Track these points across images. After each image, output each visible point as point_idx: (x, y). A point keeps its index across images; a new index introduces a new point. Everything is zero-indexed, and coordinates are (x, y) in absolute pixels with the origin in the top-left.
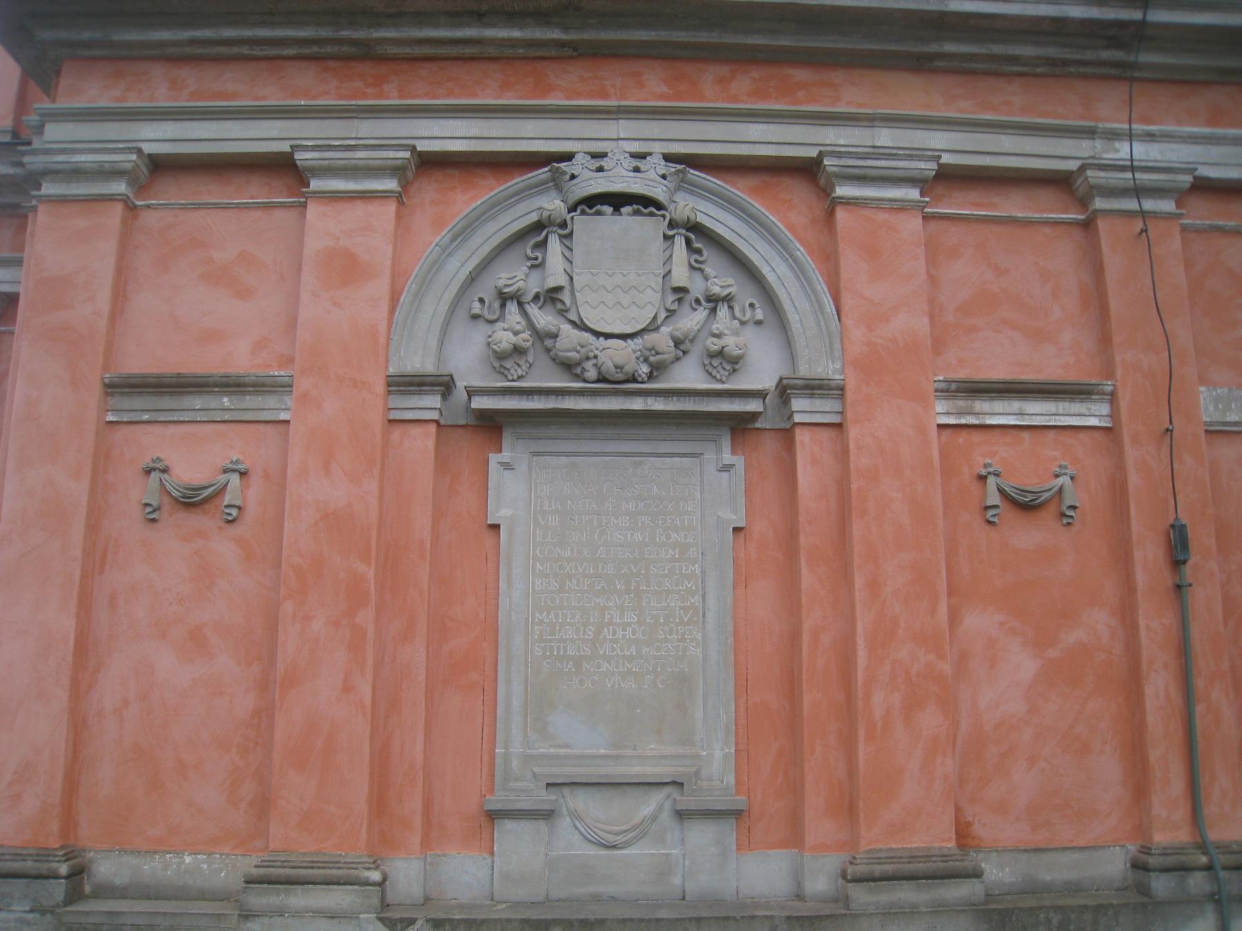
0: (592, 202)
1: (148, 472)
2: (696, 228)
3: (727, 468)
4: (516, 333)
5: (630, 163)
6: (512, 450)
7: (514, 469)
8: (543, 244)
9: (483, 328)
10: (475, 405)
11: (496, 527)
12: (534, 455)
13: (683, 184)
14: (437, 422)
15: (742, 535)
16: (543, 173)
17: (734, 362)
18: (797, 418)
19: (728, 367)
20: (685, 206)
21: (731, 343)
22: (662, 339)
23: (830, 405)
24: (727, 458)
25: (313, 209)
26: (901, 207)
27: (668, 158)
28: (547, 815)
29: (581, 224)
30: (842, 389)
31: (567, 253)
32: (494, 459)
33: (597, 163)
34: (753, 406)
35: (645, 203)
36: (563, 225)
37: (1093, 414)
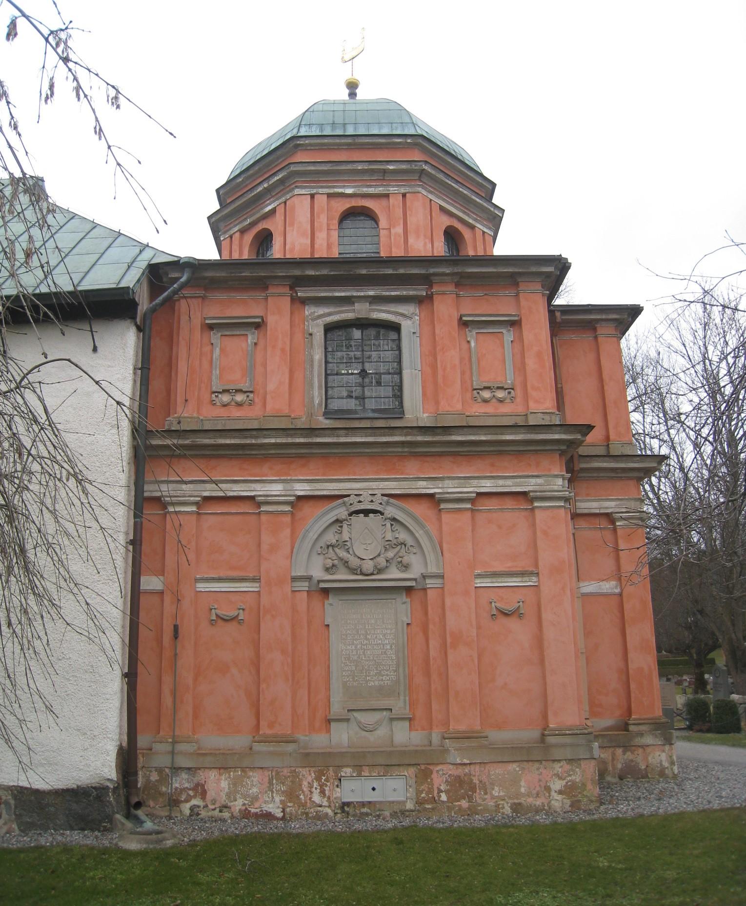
0: (358, 512)
2: (394, 519)
4: (333, 560)
5: (370, 498)
6: (332, 599)
8: (341, 527)
9: (322, 557)
10: (320, 586)
11: (328, 626)
13: (388, 503)
14: (307, 591)
15: (410, 627)
16: (340, 501)
18: (428, 586)
20: (390, 511)
21: (406, 560)
22: (382, 561)
27: (383, 495)
28: (348, 720)
30: (443, 576)
31: (349, 530)
32: (326, 602)
33: (358, 499)
34: (413, 584)
35: (375, 512)
37: (532, 581)
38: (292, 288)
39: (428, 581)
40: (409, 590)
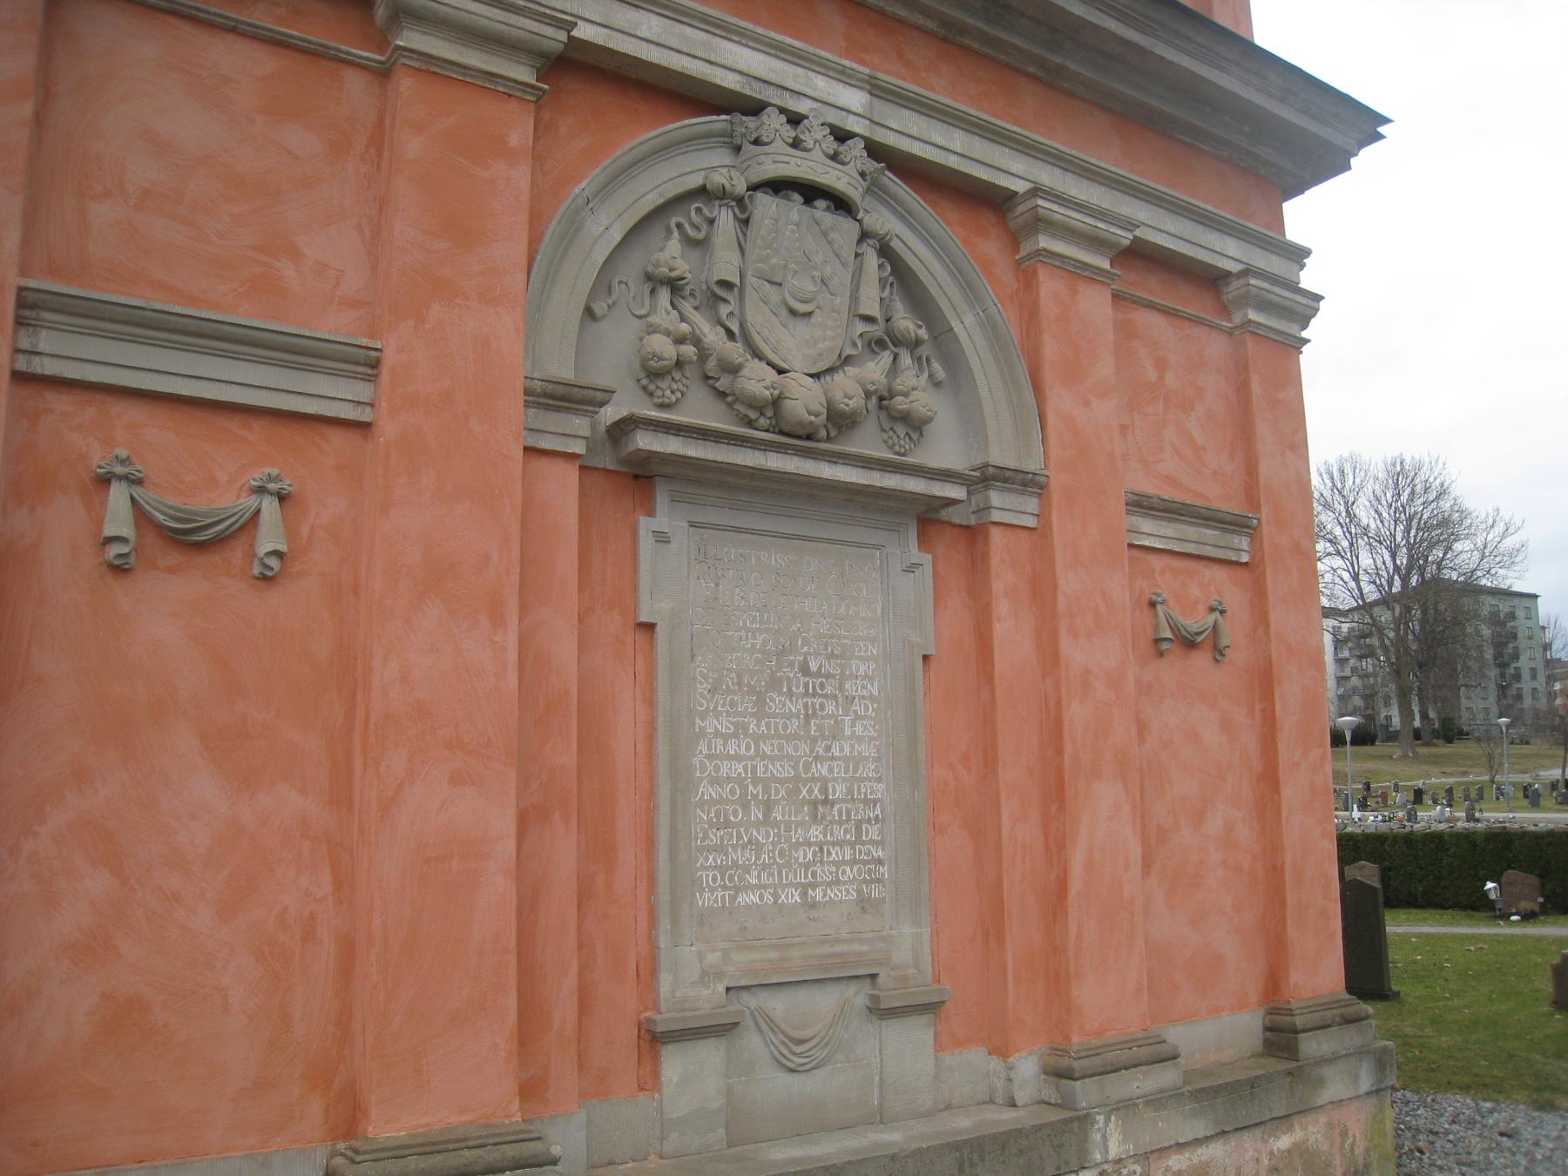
1: (1212, 610)
5: (830, 144)
7: (668, 542)
12: (691, 526)
16: (719, 121)
17: (915, 425)
18: (996, 516)
19: (915, 437)
24: (915, 554)
25: (405, 84)
29: (766, 206)
32: (646, 525)
36: (740, 201)
39: (996, 498)
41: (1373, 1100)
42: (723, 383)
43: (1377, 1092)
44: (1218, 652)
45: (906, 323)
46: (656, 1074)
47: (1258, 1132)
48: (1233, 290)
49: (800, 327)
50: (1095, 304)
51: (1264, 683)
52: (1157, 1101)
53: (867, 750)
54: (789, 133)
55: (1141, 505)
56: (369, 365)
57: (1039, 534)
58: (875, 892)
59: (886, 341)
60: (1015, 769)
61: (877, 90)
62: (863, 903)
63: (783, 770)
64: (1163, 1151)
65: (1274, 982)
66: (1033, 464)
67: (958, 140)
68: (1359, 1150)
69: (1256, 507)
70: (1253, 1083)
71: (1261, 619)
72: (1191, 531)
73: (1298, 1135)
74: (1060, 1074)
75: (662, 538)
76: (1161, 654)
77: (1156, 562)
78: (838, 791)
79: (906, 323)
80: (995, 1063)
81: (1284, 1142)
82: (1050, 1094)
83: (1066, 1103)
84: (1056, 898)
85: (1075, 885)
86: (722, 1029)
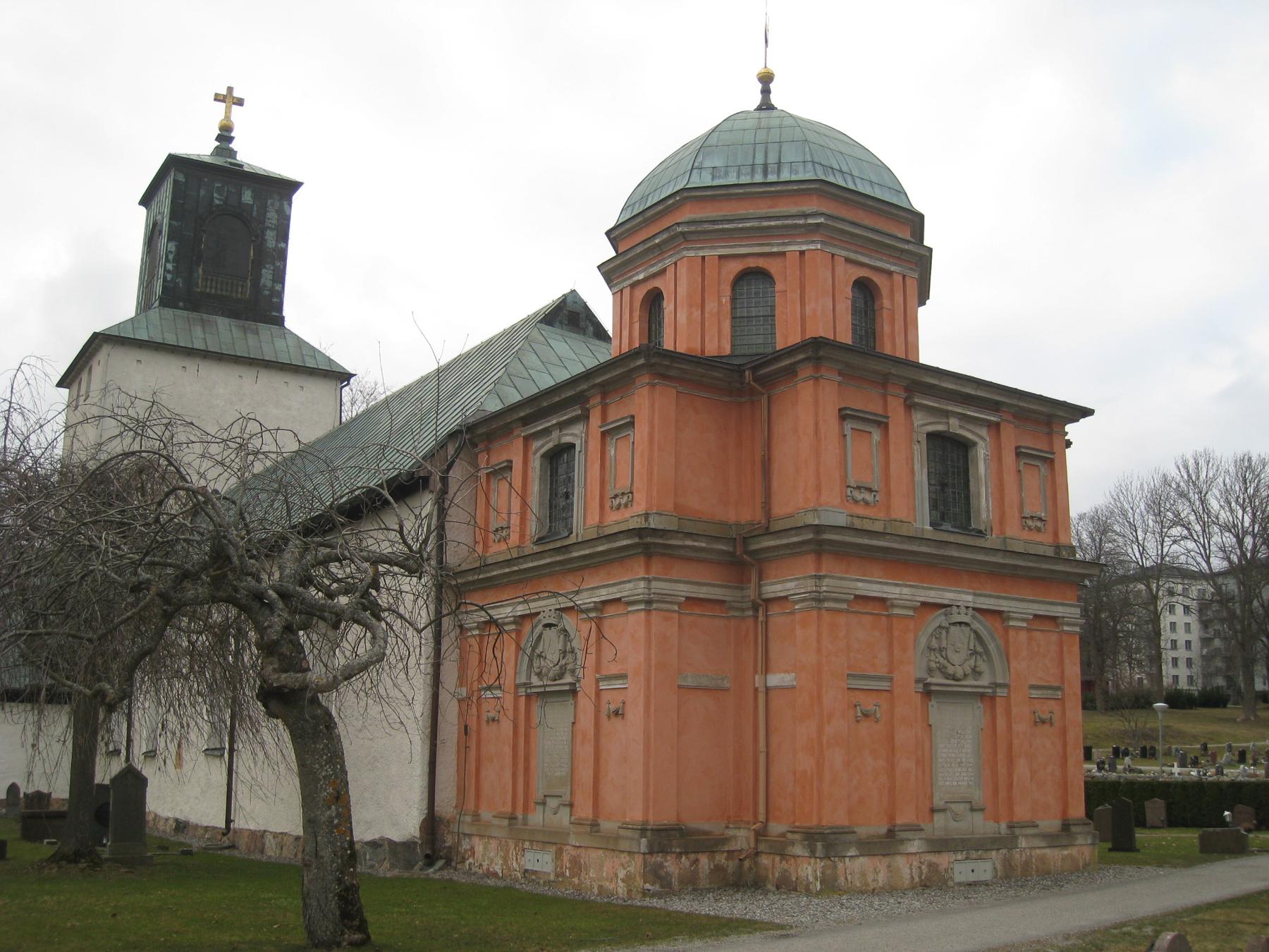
0: (954, 624)
3: (979, 707)
18: (998, 694)
23: (1006, 690)
24: (979, 704)
26: (1021, 628)
29: (953, 629)
32: (930, 704)
35: (967, 624)
38: (907, 389)
39: (998, 690)
40: (982, 696)
41: (1091, 847)
42: (943, 670)
43: (1093, 844)
44: (1051, 724)
45: (980, 649)
46: (932, 818)
47: (1059, 848)
48: (1060, 621)
49: (957, 655)
50: (1023, 636)
51: (1064, 732)
52: (1034, 836)
53: (969, 751)
54: (957, 611)
55: (1033, 687)
56: (891, 679)
57: (1008, 698)
58: (971, 783)
59: (974, 653)
60: (1001, 756)
61: (975, 595)
62: (969, 786)
63: (953, 755)
64: (1035, 848)
65: (1064, 812)
66: (1007, 682)
67: (992, 601)
68: (1087, 858)
69: (1063, 682)
70: (1058, 835)
71: (1064, 713)
72: (1045, 692)
73: (1069, 851)
74: (1011, 827)
75: (932, 706)
76: (1036, 725)
77: (1036, 701)
78: (964, 760)
79: (980, 649)
80: (996, 824)
81: (1066, 852)
82: (1009, 832)
83: (1013, 833)
84: (1010, 786)
85: (1015, 783)
86: (943, 810)
